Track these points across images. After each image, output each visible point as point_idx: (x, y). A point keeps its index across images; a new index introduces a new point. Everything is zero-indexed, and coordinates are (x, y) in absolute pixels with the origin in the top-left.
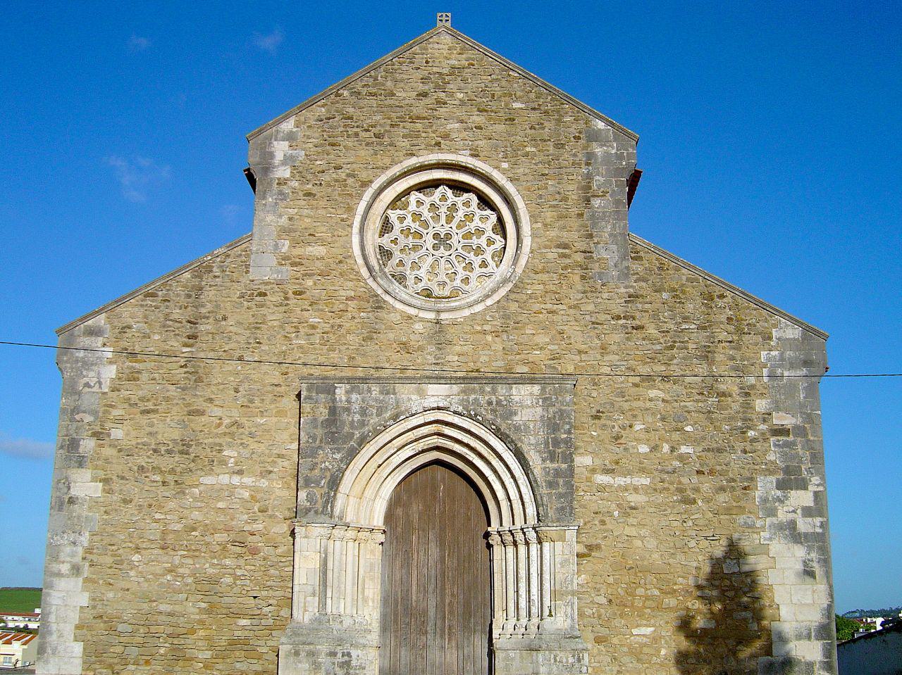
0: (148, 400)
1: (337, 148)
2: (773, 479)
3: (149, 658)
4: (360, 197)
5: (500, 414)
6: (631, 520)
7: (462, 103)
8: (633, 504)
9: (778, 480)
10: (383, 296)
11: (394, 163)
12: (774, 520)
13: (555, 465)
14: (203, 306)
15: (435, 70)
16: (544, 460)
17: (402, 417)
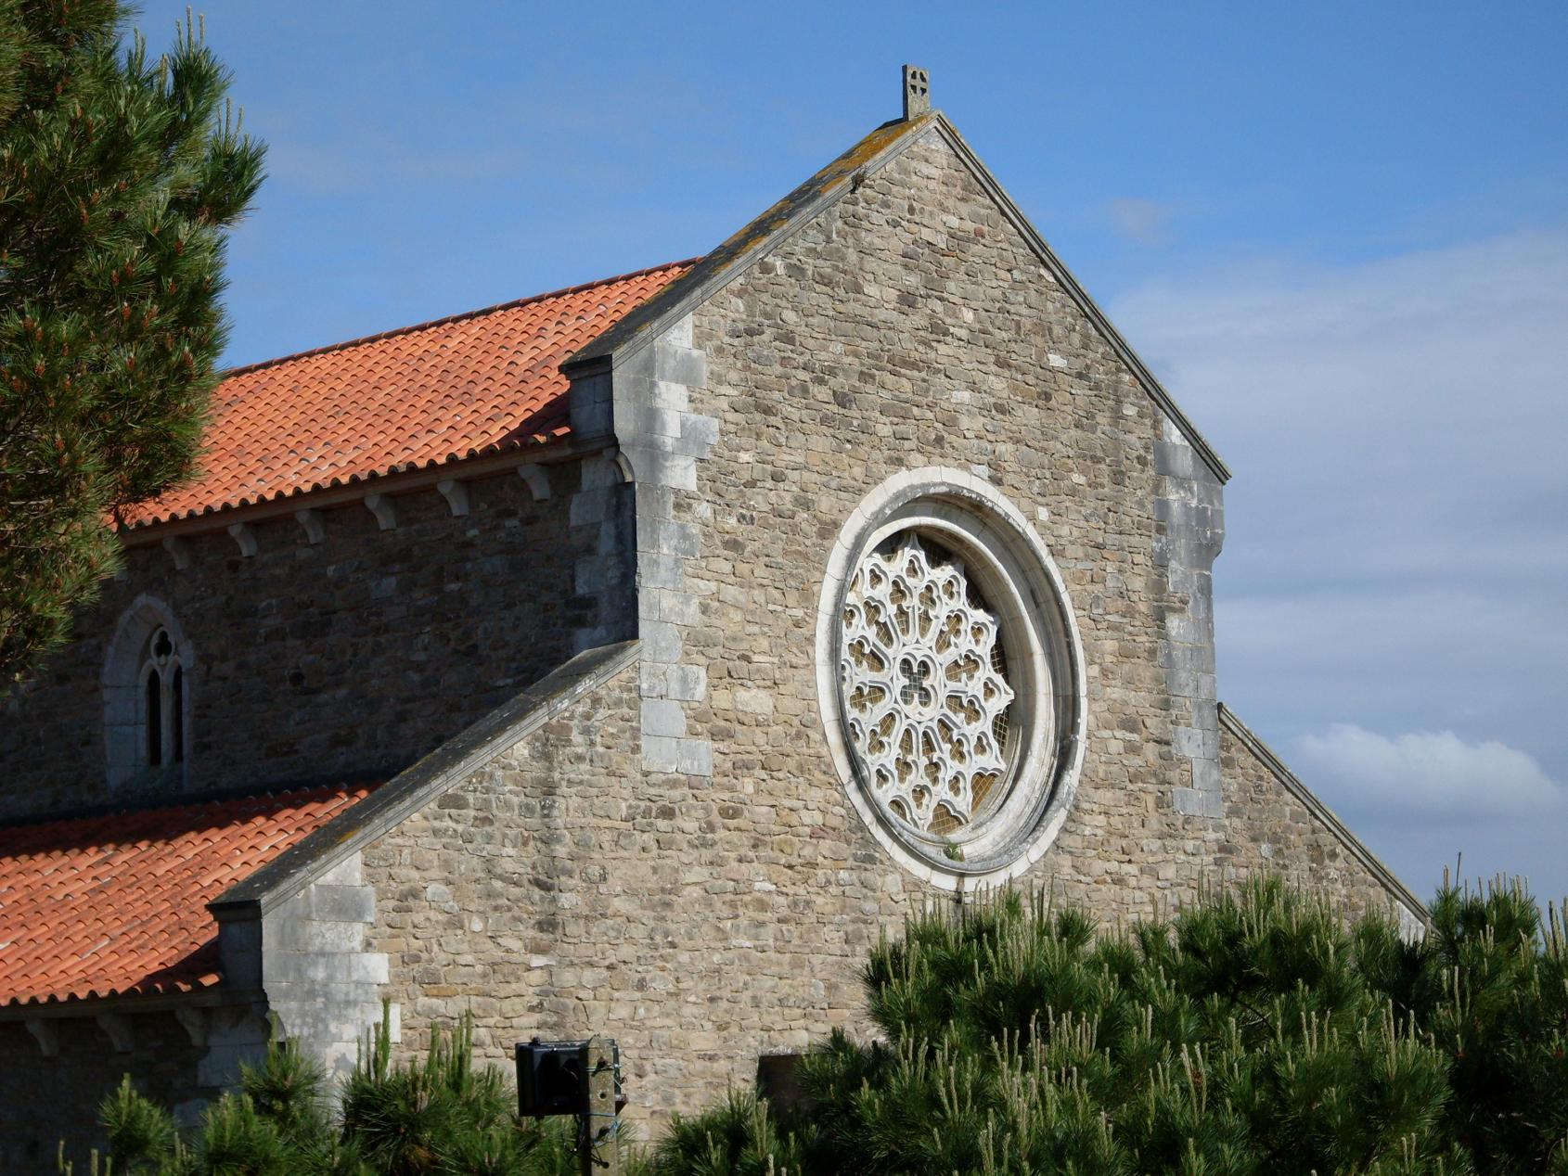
4: (821, 566)
11: (873, 480)
15: (926, 234)
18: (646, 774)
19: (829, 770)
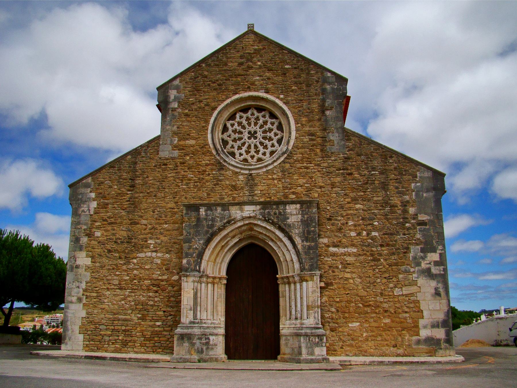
0: (112, 218)
1: (200, 92)
2: (419, 247)
3: (114, 341)
4: (211, 115)
5: (281, 219)
6: (347, 270)
7: (260, 67)
8: (348, 262)
9: (421, 248)
10: (223, 163)
11: (227, 98)
12: (420, 268)
13: (308, 244)
14: (137, 172)
15: (247, 51)
16: (303, 241)
17: (233, 222)
18: (160, 158)
19: (211, 153)
